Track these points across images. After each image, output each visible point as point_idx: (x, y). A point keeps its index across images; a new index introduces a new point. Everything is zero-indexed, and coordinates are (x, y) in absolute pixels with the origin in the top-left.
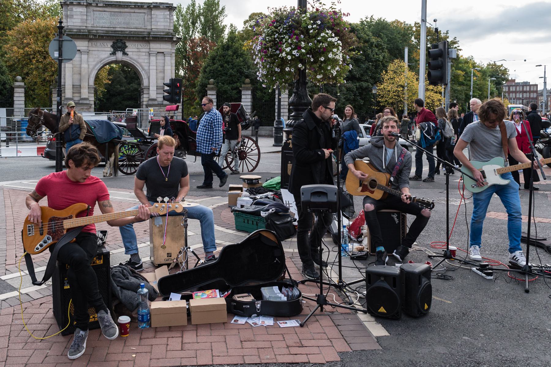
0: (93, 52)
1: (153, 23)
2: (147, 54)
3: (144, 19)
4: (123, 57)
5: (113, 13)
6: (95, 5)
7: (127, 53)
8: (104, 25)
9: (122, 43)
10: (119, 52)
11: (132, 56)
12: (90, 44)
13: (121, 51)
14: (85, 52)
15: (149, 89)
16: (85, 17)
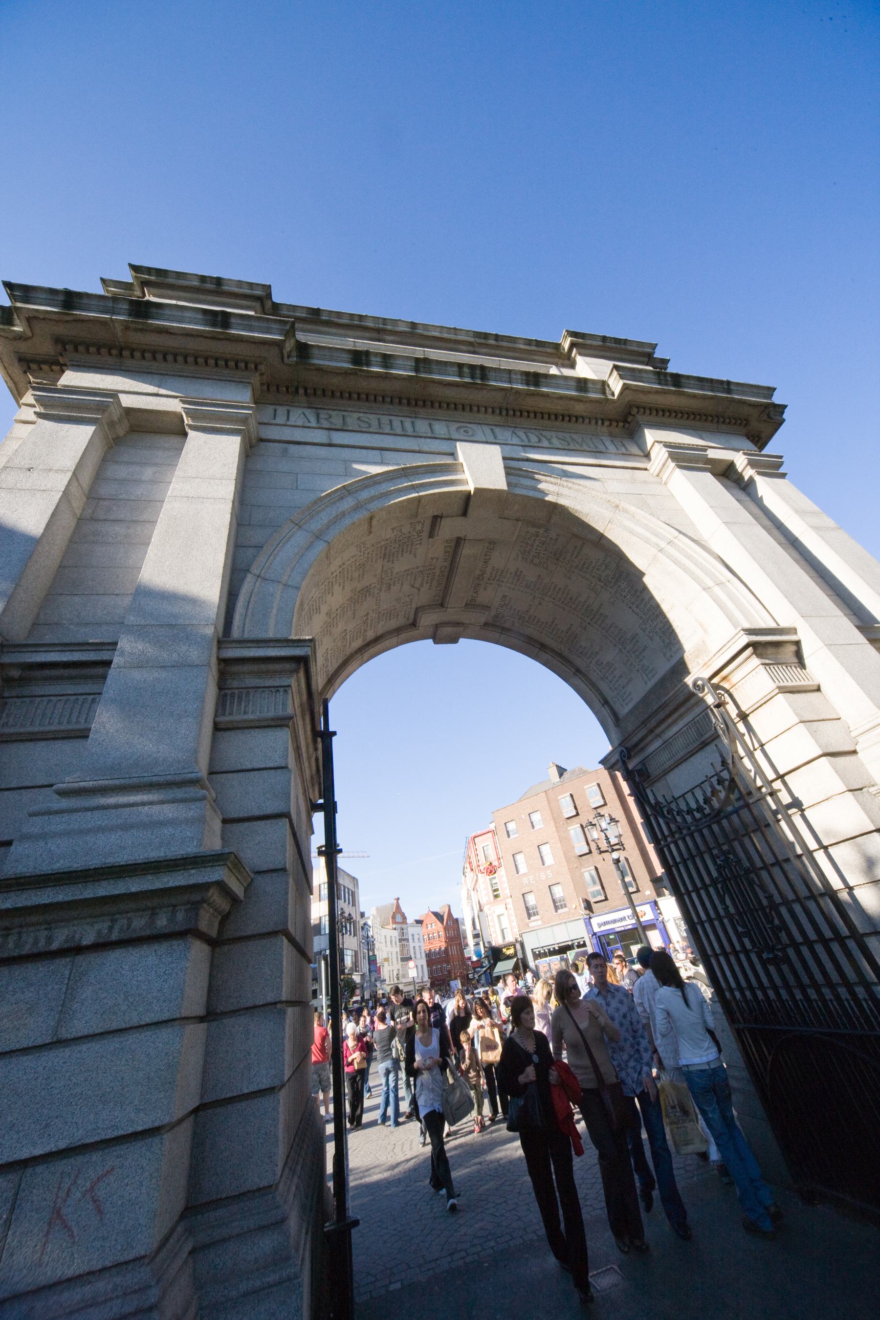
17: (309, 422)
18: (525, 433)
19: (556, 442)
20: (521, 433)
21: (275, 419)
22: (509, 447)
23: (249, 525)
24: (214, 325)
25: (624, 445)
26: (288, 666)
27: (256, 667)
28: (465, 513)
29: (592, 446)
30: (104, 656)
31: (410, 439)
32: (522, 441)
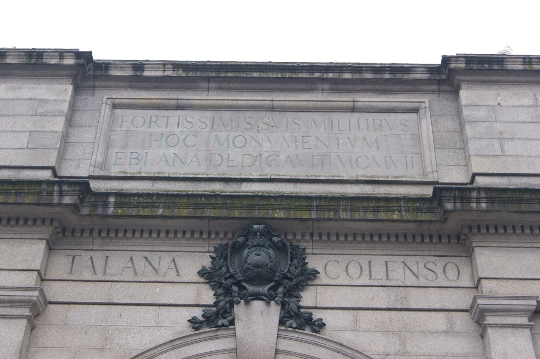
0: (75, 312)
1: (473, 147)
3: (417, 138)
4: (284, 345)
5: (227, 115)
6: (128, 73)
7: (316, 315)
8: (168, 171)
9: (281, 248)
10: (258, 305)
11: (346, 338)
13: (268, 299)
14: (12, 303)
16: (59, 124)
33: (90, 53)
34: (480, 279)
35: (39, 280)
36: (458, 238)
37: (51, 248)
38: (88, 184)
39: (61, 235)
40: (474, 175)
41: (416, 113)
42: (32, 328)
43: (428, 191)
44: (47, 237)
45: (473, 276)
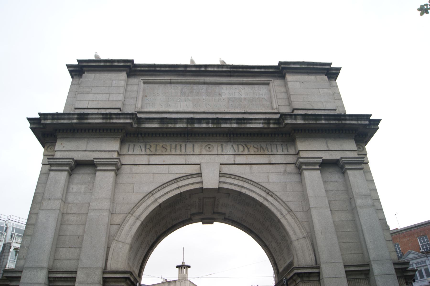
2: (291, 168)
12: (126, 147)
15: (318, 274)
17: (142, 152)
18: (238, 145)
19: (252, 151)
20: (235, 147)
21: (128, 152)
22: (228, 156)
23: (115, 214)
24: (106, 118)
25: (287, 148)
26: (123, 280)
27: (113, 280)
28: (203, 192)
29: (270, 150)
30: (73, 275)
31: (183, 156)
32: (235, 151)
33: (133, 60)
34: (299, 151)
35: (118, 155)
36: (289, 134)
37: (123, 142)
38: (136, 114)
39: (125, 136)
40: (294, 110)
41: (268, 85)
42: (117, 175)
43: (278, 116)
44: (120, 137)
45: (296, 151)
